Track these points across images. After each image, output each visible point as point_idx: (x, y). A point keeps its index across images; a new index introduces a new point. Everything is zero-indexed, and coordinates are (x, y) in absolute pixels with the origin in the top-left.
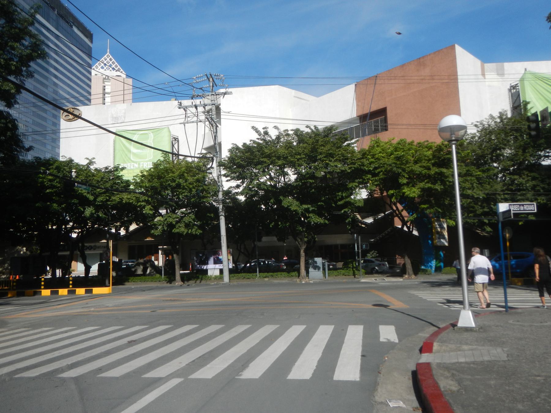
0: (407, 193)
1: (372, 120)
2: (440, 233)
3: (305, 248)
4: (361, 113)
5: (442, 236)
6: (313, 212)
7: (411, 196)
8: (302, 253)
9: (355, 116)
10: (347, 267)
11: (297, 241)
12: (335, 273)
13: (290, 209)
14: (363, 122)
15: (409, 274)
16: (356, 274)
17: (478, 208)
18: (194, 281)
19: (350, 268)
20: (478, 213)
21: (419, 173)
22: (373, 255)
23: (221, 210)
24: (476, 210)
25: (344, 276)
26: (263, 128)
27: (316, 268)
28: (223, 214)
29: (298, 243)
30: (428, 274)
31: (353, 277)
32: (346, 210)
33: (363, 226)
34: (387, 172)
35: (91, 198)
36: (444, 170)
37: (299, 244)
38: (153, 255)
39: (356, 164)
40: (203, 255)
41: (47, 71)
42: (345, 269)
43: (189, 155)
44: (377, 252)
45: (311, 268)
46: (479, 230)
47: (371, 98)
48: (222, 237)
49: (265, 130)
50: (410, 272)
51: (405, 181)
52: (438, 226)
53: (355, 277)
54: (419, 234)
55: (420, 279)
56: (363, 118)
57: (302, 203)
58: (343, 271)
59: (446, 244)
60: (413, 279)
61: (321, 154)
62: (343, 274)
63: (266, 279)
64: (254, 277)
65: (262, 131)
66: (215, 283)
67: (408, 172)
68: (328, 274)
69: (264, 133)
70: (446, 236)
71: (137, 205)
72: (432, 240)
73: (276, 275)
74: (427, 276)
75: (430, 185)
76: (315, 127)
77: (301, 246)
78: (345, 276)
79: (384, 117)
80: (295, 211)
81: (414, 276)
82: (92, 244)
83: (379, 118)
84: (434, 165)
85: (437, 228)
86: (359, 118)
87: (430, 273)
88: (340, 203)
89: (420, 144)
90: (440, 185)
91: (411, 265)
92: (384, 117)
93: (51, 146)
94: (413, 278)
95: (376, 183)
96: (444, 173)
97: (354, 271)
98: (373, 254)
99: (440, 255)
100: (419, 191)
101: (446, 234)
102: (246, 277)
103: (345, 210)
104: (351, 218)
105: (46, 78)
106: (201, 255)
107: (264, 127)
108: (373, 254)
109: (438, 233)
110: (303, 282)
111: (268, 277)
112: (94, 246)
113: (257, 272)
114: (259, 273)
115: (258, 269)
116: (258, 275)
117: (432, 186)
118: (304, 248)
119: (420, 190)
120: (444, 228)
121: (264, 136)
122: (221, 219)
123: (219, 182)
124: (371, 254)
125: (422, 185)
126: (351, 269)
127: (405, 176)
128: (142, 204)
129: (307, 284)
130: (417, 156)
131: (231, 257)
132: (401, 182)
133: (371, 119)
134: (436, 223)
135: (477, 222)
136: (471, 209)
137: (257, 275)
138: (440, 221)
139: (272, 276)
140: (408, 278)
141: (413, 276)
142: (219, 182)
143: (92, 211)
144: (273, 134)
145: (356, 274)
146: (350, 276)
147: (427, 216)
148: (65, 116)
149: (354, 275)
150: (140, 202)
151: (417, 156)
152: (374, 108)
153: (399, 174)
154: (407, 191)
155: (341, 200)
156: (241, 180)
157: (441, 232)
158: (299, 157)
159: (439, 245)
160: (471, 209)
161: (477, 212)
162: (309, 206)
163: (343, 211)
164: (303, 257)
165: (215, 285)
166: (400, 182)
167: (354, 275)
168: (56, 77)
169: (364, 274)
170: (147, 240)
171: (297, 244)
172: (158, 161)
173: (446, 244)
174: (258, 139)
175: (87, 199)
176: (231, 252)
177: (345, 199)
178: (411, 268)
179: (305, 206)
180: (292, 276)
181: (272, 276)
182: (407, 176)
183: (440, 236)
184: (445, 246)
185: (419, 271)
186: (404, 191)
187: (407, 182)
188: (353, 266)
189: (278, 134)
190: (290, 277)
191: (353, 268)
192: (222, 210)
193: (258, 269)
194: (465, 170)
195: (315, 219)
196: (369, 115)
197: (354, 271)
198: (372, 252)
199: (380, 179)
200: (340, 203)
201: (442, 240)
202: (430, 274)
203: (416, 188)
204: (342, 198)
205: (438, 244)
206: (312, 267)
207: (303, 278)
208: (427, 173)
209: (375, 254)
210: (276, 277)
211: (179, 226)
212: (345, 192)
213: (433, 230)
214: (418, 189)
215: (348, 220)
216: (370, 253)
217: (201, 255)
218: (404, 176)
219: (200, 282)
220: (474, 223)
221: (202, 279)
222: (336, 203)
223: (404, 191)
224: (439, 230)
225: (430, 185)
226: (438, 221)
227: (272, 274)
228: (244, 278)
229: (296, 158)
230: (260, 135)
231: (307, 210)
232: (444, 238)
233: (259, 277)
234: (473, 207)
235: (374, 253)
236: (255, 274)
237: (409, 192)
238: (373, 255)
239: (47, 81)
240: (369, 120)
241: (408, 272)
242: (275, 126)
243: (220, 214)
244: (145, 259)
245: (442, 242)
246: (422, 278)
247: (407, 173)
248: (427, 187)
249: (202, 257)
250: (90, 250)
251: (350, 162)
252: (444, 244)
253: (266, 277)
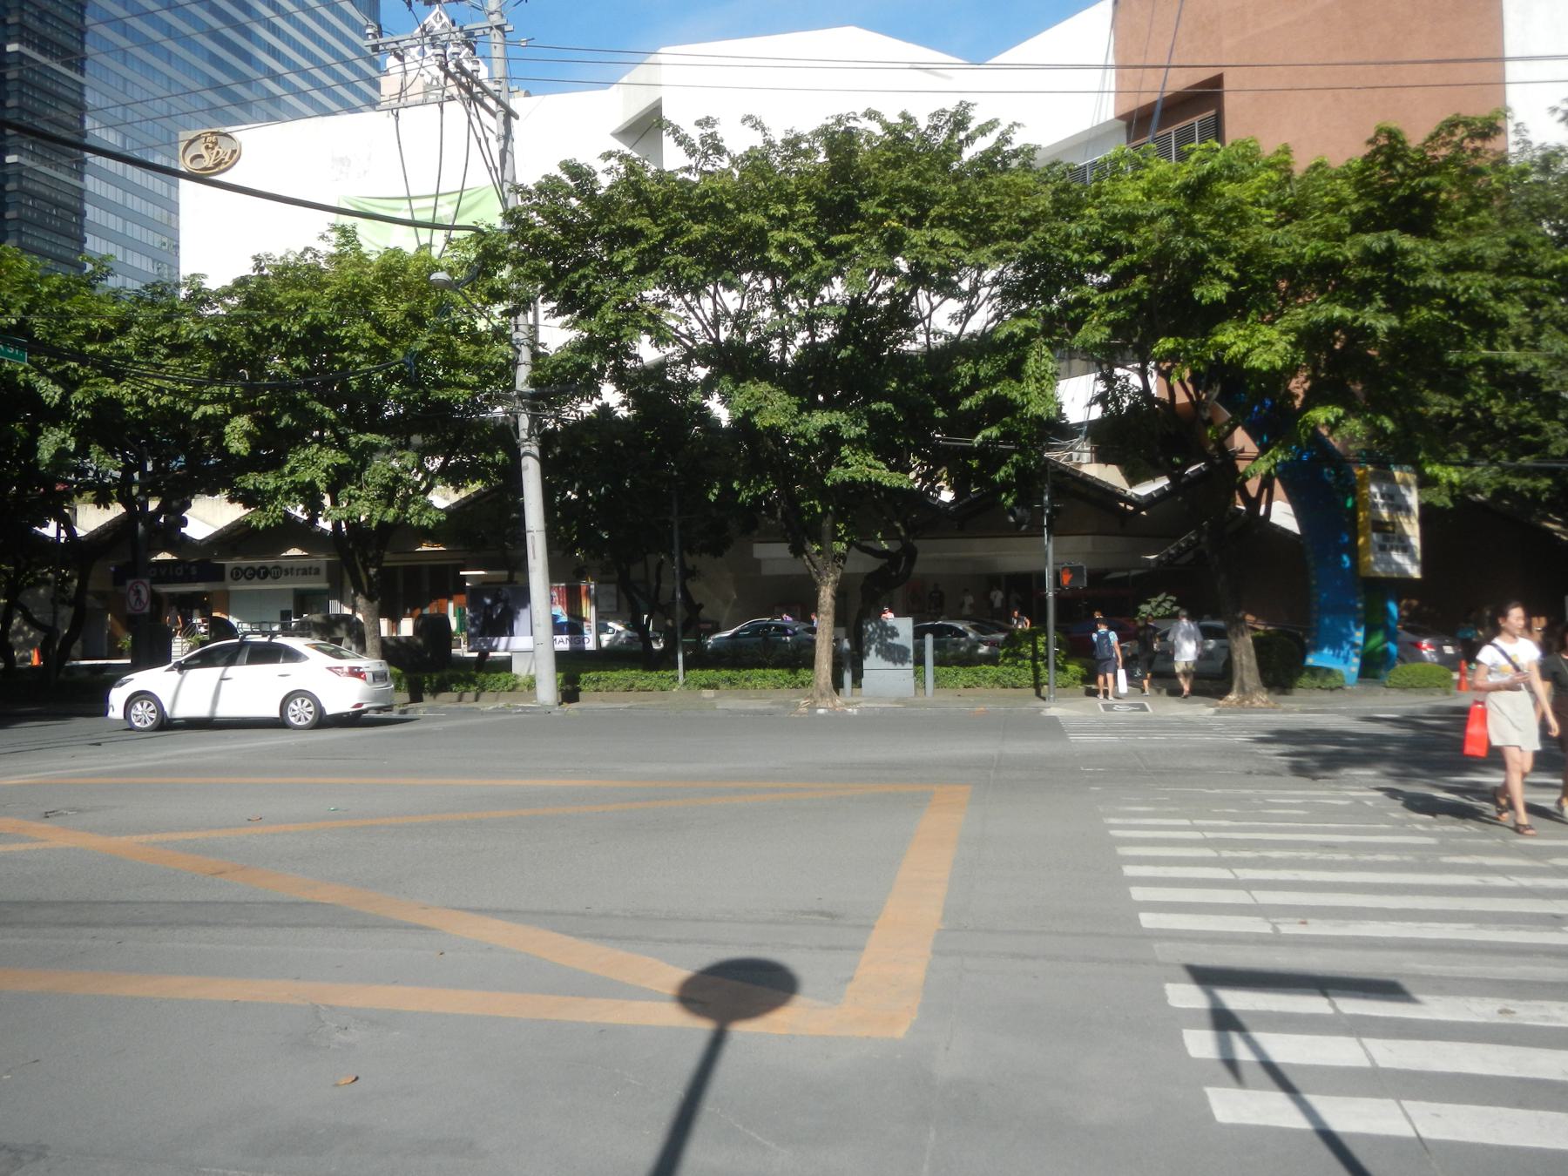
0: (1235, 349)
1: (1172, 129)
2: (1390, 528)
3: (836, 581)
4: (1132, 103)
5: (1392, 537)
6: (859, 443)
7: (1256, 364)
8: (826, 596)
9: (1111, 115)
10: (1012, 655)
11: (806, 552)
12: (964, 675)
13: (755, 424)
14: (1137, 137)
15: (1242, 689)
16: (1042, 681)
17: (1555, 431)
18: (455, 696)
19: (1023, 657)
20: (1556, 453)
21: (1290, 261)
22: (1161, 610)
23: (523, 435)
24: (1547, 443)
25: (998, 690)
26: (699, 123)
27: (894, 654)
28: (535, 450)
29: (809, 558)
30: (1331, 689)
31: (1033, 691)
32: (993, 432)
33: (1130, 508)
34: (953, 115)
35: (51, 392)
36: (1406, 242)
37: (815, 566)
38: (450, 598)
39: (1030, 237)
40: (496, 600)
41: (247, 58)
42: (1007, 661)
43: (419, 230)
44: (1174, 599)
45: (872, 652)
46: (1555, 522)
47: (1169, 44)
48: (529, 536)
49: (709, 131)
50: (1246, 679)
51: (1219, 291)
52: (1379, 500)
53: (1038, 694)
54: (1301, 529)
55: (1286, 711)
56: (1138, 122)
57: (809, 407)
58: (993, 671)
59: (1415, 572)
60: (1259, 710)
61: (874, 192)
62: (997, 680)
63: (708, 694)
64: (665, 684)
65: (695, 134)
66: (501, 705)
67: (1240, 255)
68: (936, 680)
69: (703, 143)
70: (1415, 541)
71: (192, 413)
72: (1354, 552)
73: (747, 680)
74: (1326, 696)
75: (1337, 311)
76: (904, 116)
77: (819, 574)
78: (1004, 687)
79: (1213, 112)
80: (774, 432)
81: (1265, 698)
82: (256, 563)
83: (1196, 120)
84: (1360, 224)
85: (1375, 505)
86: (1123, 123)
87: (1339, 684)
88: (967, 404)
89: (1320, 169)
90: (1385, 311)
91: (1252, 652)
92: (1213, 112)
93: (150, 261)
94: (1258, 704)
95: (1111, 316)
96: (1405, 253)
97: (1036, 670)
98: (1159, 605)
99: (1386, 611)
100: (1291, 343)
101: (1412, 530)
102: (638, 684)
103: (987, 432)
104: (1014, 465)
105: (247, 81)
106: (488, 601)
107: (702, 116)
108: (1159, 605)
109: (1379, 526)
110: (821, 711)
111: (714, 686)
112: (276, 567)
113: (676, 667)
114: (687, 667)
115: (680, 657)
116: (681, 677)
117: (1349, 314)
118: (832, 578)
119: (1292, 337)
120: (1408, 510)
121: (706, 156)
122: (527, 468)
123: (517, 330)
124: (1154, 604)
125: (1299, 316)
126: (1028, 662)
127: (1224, 273)
128: (210, 410)
129: (839, 725)
130: (1292, 195)
131: (593, 609)
132: (1202, 297)
133: (1164, 124)
134: (1374, 489)
135: (1548, 489)
136: (1528, 437)
137: (676, 679)
138: (1391, 479)
139: (731, 681)
140: (1241, 707)
141: (1262, 698)
142: (517, 330)
143: (64, 441)
144: (739, 141)
145: (1042, 681)
146: (1020, 687)
147: (1338, 462)
148: (192, 160)
149: (1037, 686)
150: (205, 403)
151: (1292, 195)
152: (1180, 81)
153: (1197, 267)
154: (1231, 338)
155: (968, 392)
156: (433, 277)
157: (1393, 523)
158: (782, 210)
159: (1383, 575)
160: (1528, 437)
161: (1551, 447)
162: (838, 417)
163: (979, 437)
164: (826, 614)
165: (503, 711)
166: (1197, 297)
167: (1037, 686)
168: (275, 77)
169: (1079, 682)
170: (424, 548)
171: (808, 563)
172: (302, 254)
173: (1415, 572)
174: (688, 169)
175: (31, 394)
176: (593, 592)
177: (987, 386)
178: (1254, 663)
179: (820, 419)
180: (803, 683)
181: (733, 684)
182: (1228, 269)
183: (1386, 539)
184: (1411, 581)
185: (1300, 674)
186: (1219, 338)
187: (1229, 295)
188: (1035, 650)
189: (760, 144)
190: (796, 687)
191: (1034, 659)
192: (530, 435)
193: (680, 657)
194: (1502, 240)
195: (861, 467)
196: (1159, 107)
197: (1036, 670)
198: (1160, 599)
199: (1126, 298)
200: (967, 404)
201: (1397, 557)
202: (1340, 687)
203: (1279, 328)
204: (977, 383)
205: (1379, 570)
206: (878, 652)
207: (822, 695)
208: (1326, 253)
209: (1167, 605)
210: (744, 687)
211: (351, 497)
212: (989, 360)
213: (1361, 514)
214: (1284, 333)
215: (1002, 473)
216: (1149, 603)
217: (488, 601)
218: (1217, 273)
219: (477, 699)
220: (1534, 491)
221: (483, 689)
222: (950, 402)
223: (1219, 338)
224: (1385, 513)
225: (1337, 311)
226: (1384, 476)
227: (726, 673)
228: (632, 686)
229: (771, 218)
230: (691, 155)
231: (831, 437)
232: (1406, 548)
233: (685, 684)
234: (1536, 430)
235: (1164, 601)
236: (669, 673)
237: (1242, 346)
238: (1161, 610)
239: (250, 88)
240: (1159, 129)
241: (1242, 680)
242: (750, 118)
243: (523, 450)
244: (427, 611)
245: (1398, 564)
246: (1297, 706)
247: (1231, 260)
248: (1320, 317)
249: (491, 607)
250: (248, 579)
251: (1002, 228)
252: (1406, 572)
253: (708, 686)
